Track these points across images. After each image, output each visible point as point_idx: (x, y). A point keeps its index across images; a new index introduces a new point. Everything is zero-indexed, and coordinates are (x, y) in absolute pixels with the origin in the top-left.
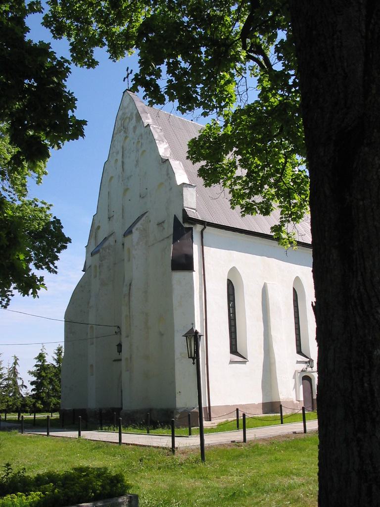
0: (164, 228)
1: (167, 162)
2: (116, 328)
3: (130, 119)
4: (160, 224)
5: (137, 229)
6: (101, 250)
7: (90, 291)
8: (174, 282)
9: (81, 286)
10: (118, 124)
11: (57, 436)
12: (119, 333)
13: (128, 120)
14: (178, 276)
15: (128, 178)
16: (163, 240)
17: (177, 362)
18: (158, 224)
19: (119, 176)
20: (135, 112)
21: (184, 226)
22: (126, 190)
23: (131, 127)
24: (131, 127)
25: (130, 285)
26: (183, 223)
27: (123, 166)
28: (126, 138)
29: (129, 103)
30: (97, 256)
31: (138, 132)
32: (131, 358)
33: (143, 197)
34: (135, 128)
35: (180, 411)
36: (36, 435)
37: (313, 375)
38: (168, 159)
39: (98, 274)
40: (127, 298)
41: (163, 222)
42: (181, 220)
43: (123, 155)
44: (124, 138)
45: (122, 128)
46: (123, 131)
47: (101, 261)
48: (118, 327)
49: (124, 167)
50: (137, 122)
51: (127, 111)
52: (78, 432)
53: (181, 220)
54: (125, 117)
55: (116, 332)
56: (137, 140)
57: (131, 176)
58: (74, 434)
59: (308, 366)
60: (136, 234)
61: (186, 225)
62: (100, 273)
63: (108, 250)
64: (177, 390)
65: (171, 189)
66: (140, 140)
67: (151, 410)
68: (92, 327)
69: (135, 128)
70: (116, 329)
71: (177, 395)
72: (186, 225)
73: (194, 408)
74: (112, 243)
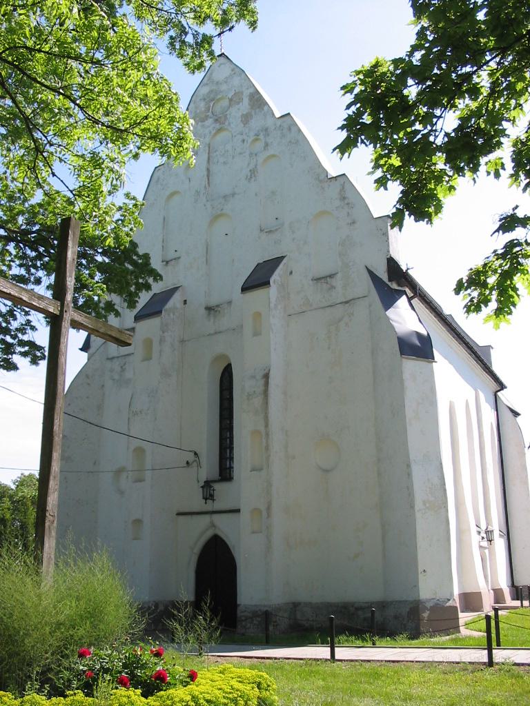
0: (333, 287)
1: (341, 180)
3: (235, 100)
4: (325, 279)
5: (274, 282)
6: (163, 312)
7: (103, 386)
8: (406, 376)
9: (87, 376)
10: (196, 108)
11: (268, 658)
12: (195, 464)
13: (225, 103)
14: (411, 365)
15: (225, 197)
16: (331, 306)
17: (418, 515)
18: (318, 279)
19: (198, 193)
20: (247, 92)
21: (392, 287)
22: (216, 218)
23: (236, 113)
24: (236, 113)
25: (266, 376)
26: (390, 280)
27: (208, 176)
28: (220, 130)
29: (231, 75)
30: (154, 322)
31: (256, 123)
32: (269, 508)
33: (270, 231)
34: (246, 119)
35: (429, 605)
36: (219, 659)
39: (155, 355)
40: (257, 401)
41: (331, 276)
42: (383, 274)
43: (209, 159)
44: (213, 132)
45: (210, 114)
46: (210, 121)
47: (163, 332)
48: (196, 454)
49: (210, 178)
50: (252, 108)
51: (224, 87)
52: (329, 648)
53: (385, 277)
54: (219, 97)
55: (188, 463)
56: (253, 138)
57: (233, 194)
58: (323, 652)
59: (483, 538)
60: (273, 290)
61: (394, 286)
62: (161, 351)
63: (172, 315)
64: (420, 570)
65: (354, 223)
66: (261, 137)
67: (295, 605)
68: (140, 452)
69: (246, 119)
70: (191, 457)
71: (421, 577)
72: (394, 286)
73: (449, 600)
74: (179, 305)
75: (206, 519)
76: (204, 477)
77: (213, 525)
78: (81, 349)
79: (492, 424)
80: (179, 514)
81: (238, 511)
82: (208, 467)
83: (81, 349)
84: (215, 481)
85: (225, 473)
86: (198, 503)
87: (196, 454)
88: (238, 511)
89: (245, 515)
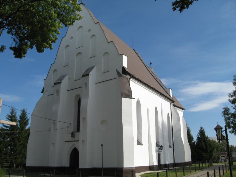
2: (69, 124)
14: (124, 100)
37: (160, 154)
38: (112, 41)
42: (121, 72)
48: (70, 124)
75: (72, 143)
76: (72, 131)
77: (74, 145)
78: (41, 92)
79: (168, 113)
80: (65, 141)
81: (79, 141)
82: (72, 129)
83: (41, 92)
84: (75, 132)
85: (78, 130)
86: (69, 138)
87: (70, 124)
88: (79, 141)
89: (80, 142)
